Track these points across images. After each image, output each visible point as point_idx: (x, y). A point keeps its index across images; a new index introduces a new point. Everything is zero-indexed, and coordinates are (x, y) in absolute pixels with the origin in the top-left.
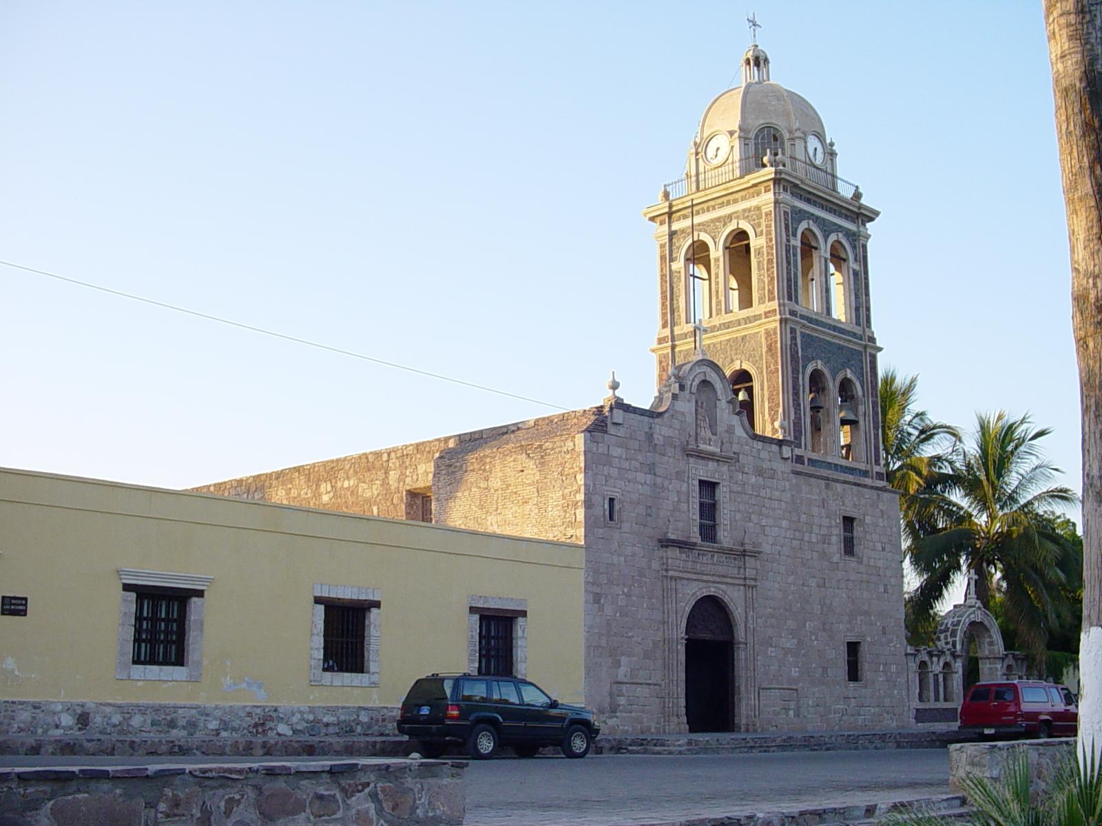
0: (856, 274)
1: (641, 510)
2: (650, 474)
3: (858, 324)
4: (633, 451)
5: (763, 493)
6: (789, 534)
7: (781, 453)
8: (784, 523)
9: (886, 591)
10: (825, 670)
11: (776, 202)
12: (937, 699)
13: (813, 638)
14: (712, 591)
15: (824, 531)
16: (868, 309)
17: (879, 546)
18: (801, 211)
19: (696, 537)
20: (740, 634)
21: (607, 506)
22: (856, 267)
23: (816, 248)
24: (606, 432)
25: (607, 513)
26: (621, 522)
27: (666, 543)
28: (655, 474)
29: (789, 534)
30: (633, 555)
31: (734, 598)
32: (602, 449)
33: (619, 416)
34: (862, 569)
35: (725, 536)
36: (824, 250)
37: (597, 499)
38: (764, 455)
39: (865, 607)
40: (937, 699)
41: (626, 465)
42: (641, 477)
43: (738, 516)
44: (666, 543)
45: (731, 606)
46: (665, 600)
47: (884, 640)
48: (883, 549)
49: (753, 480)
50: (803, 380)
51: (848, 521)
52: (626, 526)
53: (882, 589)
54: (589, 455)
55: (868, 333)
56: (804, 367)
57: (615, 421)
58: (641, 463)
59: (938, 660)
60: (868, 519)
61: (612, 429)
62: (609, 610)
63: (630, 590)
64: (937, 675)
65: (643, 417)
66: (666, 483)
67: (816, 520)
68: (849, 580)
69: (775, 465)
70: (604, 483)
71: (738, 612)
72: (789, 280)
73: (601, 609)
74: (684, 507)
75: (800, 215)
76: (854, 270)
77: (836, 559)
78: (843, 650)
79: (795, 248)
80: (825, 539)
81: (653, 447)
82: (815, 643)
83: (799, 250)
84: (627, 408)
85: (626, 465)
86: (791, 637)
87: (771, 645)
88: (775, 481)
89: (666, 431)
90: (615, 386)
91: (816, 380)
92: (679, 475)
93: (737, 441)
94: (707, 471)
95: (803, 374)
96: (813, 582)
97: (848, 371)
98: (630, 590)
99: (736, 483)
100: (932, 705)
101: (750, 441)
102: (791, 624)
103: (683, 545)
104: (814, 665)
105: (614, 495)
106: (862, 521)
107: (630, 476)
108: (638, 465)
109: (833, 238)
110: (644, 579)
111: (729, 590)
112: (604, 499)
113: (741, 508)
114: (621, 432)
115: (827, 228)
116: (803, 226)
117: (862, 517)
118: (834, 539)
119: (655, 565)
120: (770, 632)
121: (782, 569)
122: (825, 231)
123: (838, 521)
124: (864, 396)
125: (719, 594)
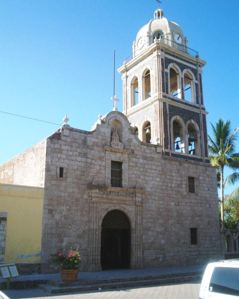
0: (196, 85)
1: (78, 173)
2: (84, 157)
3: (197, 103)
4: (75, 148)
5: (146, 167)
6: (160, 183)
7: (156, 150)
8: (158, 179)
9: (210, 207)
11: (158, 56)
13: (173, 227)
14: (117, 207)
15: (179, 182)
16: (202, 98)
17: (206, 189)
18: (170, 59)
20: (133, 226)
21: (58, 171)
22: (197, 82)
23: (178, 74)
24: (60, 139)
25: (59, 174)
26: (67, 178)
27: (91, 186)
28: (87, 158)
29: (160, 183)
30: (73, 192)
32: (57, 146)
34: (198, 198)
36: (181, 75)
37: (53, 168)
38: (148, 151)
41: (71, 153)
42: (79, 159)
43: (133, 176)
44: (91, 186)
45: (129, 215)
46: (90, 212)
48: (209, 190)
49: (141, 161)
50: (170, 122)
51: (191, 179)
52: (69, 180)
53: (208, 206)
54: (49, 149)
55: (202, 106)
57: (64, 134)
58: (79, 153)
59: (236, 234)
60: (201, 178)
62: (57, 217)
63: (70, 207)
64: (235, 240)
65: (81, 134)
66: (93, 162)
68: (191, 202)
69: (153, 155)
71: (132, 217)
72: (163, 84)
73: (53, 216)
75: (170, 61)
76: (195, 83)
77: (185, 193)
78: (189, 232)
79: (167, 73)
80: (179, 186)
81: (88, 147)
82: (174, 229)
84: (72, 130)
85: (71, 153)
86: (161, 226)
87: (150, 231)
88: (153, 162)
89: (94, 140)
90: (67, 120)
91: (176, 125)
92: (101, 158)
93: (133, 145)
94: (116, 157)
95: (170, 120)
96: (173, 204)
97: (192, 121)
98: (70, 207)
99: (132, 162)
101: (140, 145)
102: (161, 221)
103: (101, 187)
104: (173, 239)
105: (62, 166)
106: (198, 179)
107: (73, 158)
108: (77, 154)
109: (185, 71)
110: (79, 203)
111: (127, 207)
112: (57, 167)
113: (135, 172)
116: (171, 66)
117: (198, 177)
118: (184, 186)
119: (85, 196)
120: (150, 225)
121: (157, 198)
122: (182, 68)
123: (186, 178)
124: (200, 130)
125: (122, 209)
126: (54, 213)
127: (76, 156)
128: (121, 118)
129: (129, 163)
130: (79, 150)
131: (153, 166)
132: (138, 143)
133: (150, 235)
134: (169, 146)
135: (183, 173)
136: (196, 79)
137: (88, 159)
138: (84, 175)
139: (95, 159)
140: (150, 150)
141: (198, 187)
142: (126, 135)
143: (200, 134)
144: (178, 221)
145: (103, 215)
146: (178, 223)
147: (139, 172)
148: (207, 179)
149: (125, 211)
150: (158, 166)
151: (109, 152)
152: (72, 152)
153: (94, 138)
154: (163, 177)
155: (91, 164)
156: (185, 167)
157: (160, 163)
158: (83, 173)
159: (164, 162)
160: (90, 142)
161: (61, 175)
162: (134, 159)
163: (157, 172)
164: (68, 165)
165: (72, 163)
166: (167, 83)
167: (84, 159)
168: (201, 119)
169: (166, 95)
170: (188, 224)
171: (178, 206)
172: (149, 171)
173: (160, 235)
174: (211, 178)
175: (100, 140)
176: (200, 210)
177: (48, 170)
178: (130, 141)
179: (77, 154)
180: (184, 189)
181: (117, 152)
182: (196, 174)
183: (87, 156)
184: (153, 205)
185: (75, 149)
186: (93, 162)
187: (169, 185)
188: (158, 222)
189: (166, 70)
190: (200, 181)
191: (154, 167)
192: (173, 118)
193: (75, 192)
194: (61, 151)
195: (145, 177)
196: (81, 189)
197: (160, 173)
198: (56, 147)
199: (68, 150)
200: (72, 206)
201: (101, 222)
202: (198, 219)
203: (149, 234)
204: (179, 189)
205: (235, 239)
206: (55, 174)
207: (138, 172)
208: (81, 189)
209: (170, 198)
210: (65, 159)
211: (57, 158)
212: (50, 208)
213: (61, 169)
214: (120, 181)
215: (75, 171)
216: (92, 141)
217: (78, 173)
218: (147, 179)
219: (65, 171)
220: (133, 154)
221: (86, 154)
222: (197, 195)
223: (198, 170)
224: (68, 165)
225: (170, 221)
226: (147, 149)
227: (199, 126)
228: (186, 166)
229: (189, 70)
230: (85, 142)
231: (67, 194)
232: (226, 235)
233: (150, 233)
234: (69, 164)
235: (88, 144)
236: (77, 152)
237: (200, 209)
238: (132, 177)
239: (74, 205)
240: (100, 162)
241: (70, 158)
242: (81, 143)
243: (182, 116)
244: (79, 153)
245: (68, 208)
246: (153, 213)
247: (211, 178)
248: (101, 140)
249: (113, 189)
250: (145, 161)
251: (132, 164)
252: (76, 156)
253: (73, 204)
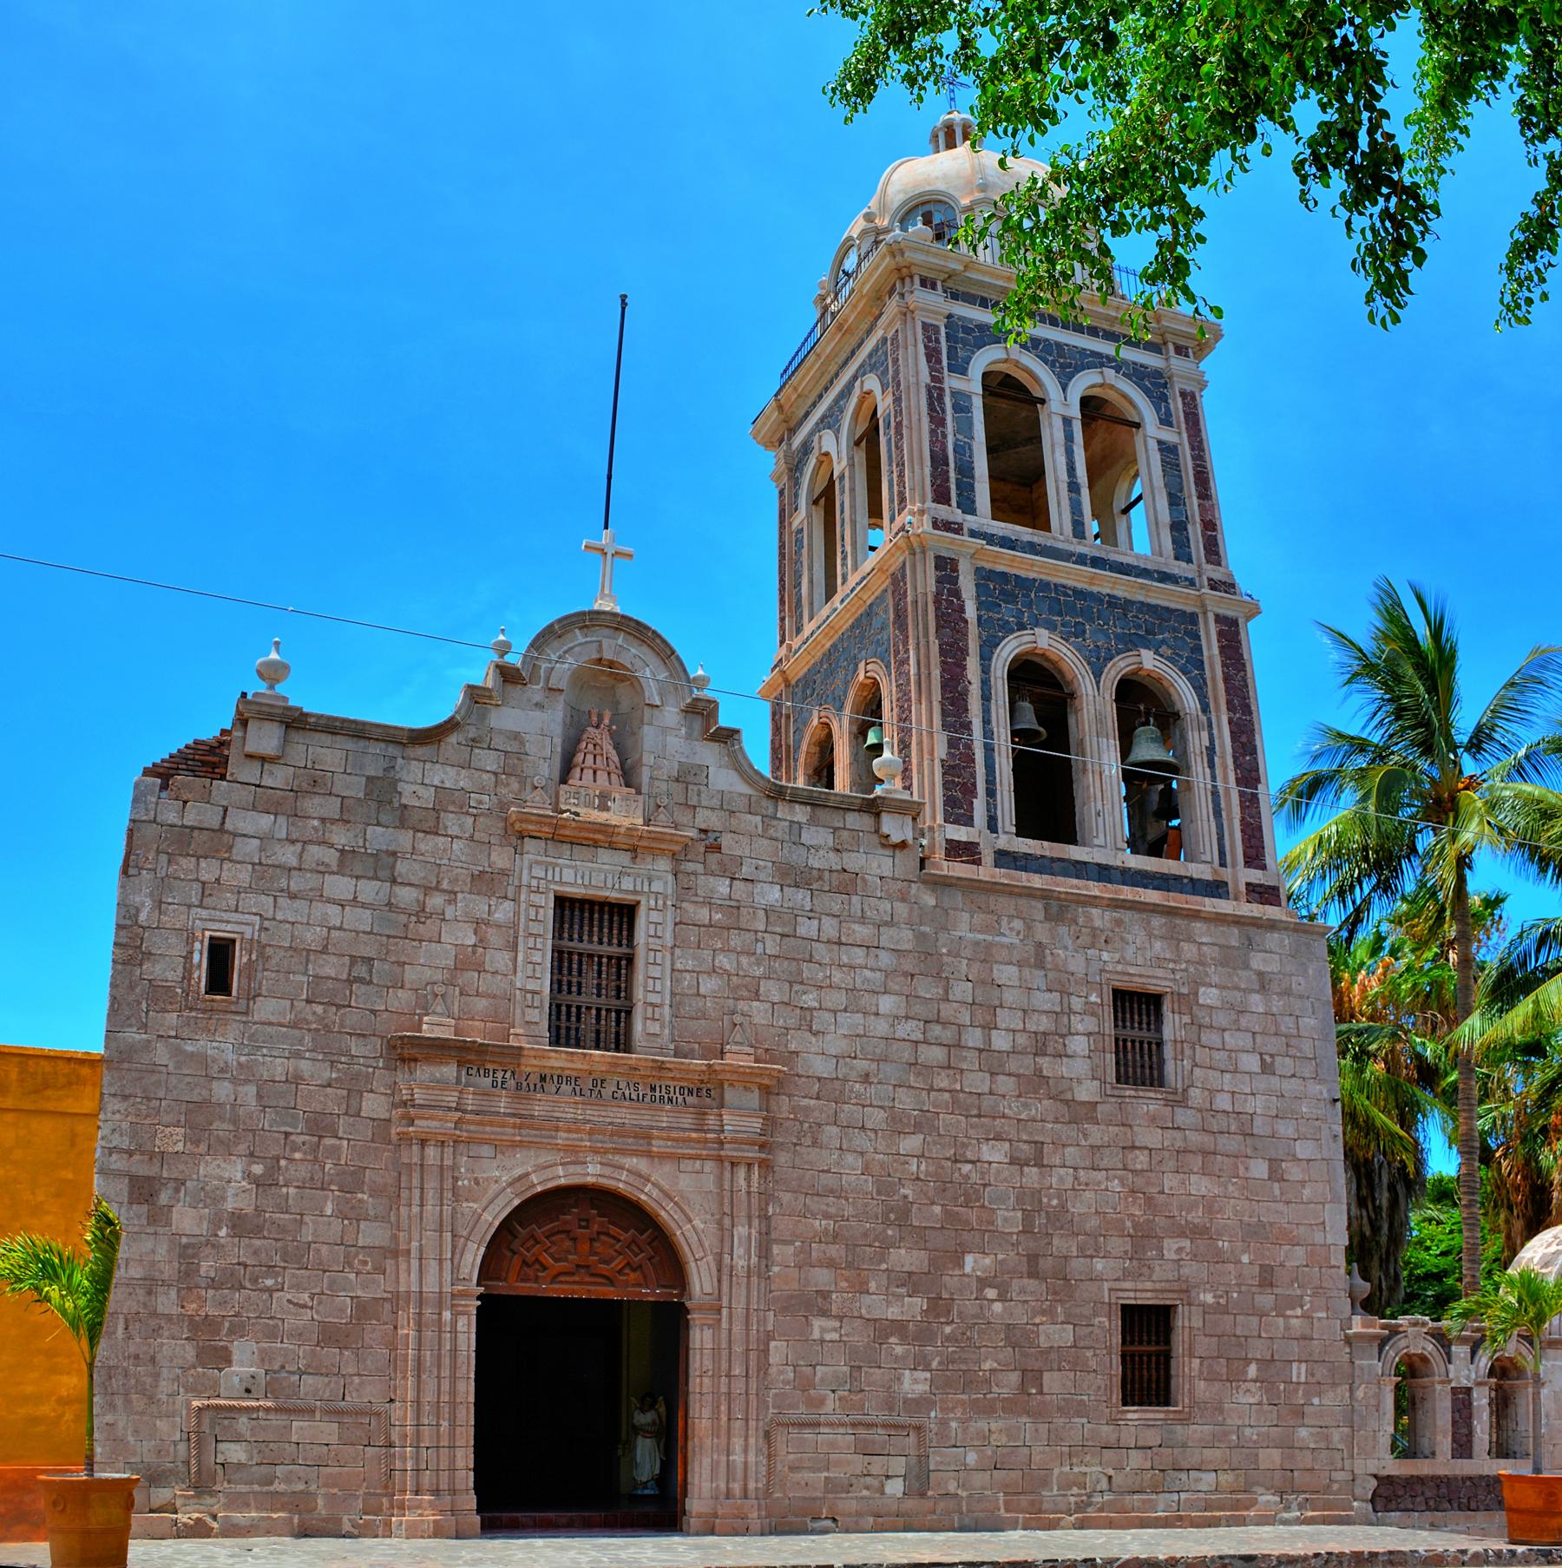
4: (316, 823)
5: (807, 928)
8: (887, 1004)
9: (1275, 1175)
10: (1031, 1377)
12: (1463, 1447)
14: (592, 1173)
16: (1210, 526)
17: (1251, 1062)
19: (529, 1026)
21: (201, 958)
22: (1168, 436)
23: (1043, 401)
26: (252, 996)
28: (394, 881)
30: (295, 1080)
31: (683, 1195)
33: (265, 738)
34: (1183, 1117)
38: (816, 836)
39: (1197, 1216)
40: (1463, 1447)
41: (288, 855)
42: (340, 886)
43: (708, 985)
45: (667, 1214)
46: (405, 1194)
47: (1265, 1300)
48: (1267, 1069)
50: (986, 670)
51: (1137, 1007)
53: (1260, 1169)
56: (988, 648)
58: (342, 851)
59: (1473, 1353)
60: (1208, 996)
61: (241, 770)
63: (273, 1165)
64: (1469, 1390)
65: (362, 743)
67: (1009, 997)
68: (1134, 1147)
69: (854, 861)
70: (195, 901)
71: (693, 1231)
74: (501, 960)
76: (1160, 442)
78: (1109, 1328)
80: (1041, 1045)
82: (998, 1307)
83: (978, 404)
84: (295, 722)
85: (288, 855)
86: (903, 1291)
87: (825, 1313)
88: (855, 899)
89: (444, 776)
92: (487, 882)
93: (715, 802)
99: (708, 903)
100: (1442, 1464)
101: (765, 803)
102: (906, 1258)
104: (987, 1365)
105: (224, 931)
106: (1187, 1002)
108: (331, 857)
110: (328, 1141)
111: (661, 1174)
113: (724, 961)
114: (277, 777)
117: (1185, 990)
118: (1078, 1045)
120: (822, 1277)
121: (877, 1117)
122: (1062, 366)
123: (1094, 998)
124: (1205, 709)
125: (621, 1183)
126: (164, 1198)
127: (322, 870)
128: (632, 654)
129: (684, 905)
130: (341, 837)
131: (856, 927)
132: (744, 789)
133: (822, 1341)
134: (979, 805)
135: (1077, 965)
136: (1166, 421)
137: (397, 889)
138: (370, 982)
139: (445, 885)
140: (836, 829)
141: (1188, 1052)
142: (665, 741)
143: (1205, 735)
144: (1033, 1259)
145: (493, 1218)
146: (1033, 1274)
147: (753, 959)
148: (1256, 1002)
149: (646, 1195)
150: (890, 923)
151: (542, 843)
152: (299, 846)
153: (448, 769)
154: (927, 989)
155: (421, 913)
156: (1093, 929)
157: (902, 909)
158: (361, 971)
159: (932, 902)
160: (421, 790)
161: (219, 980)
162: (722, 887)
163: (886, 959)
164: (266, 924)
165: (289, 910)
166: (963, 450)
167: (370, 890)
168: (1211, 649)
169: (953, 513)
170: (1113, 1281)
171: (1035, 1170)
172: (821, 951)
173: (892, 1340)
174: (1287, 992)
175: (485, 776)
176: (1203, 1191)
178: (688, 776)
179: (326, 860)
180: (1083, 1062)
181: (596, 844)
182: (1173, 971)
183: (393, 867)
184: (850, 1158)
185: (315, 828)
186: (436, 901)
187: (974, 1038)
188: (884, 1266)
189: (952, 382)
190: (1202, 1015)
191: (862, 932)
192: (1009, 649)
193: (306, 1075)
194: (219, 841)
195: (796, 987)
196: (343, 1059)
197: (908, 965)
198: (190, 819)
199: (265, 839)
200: (283, 1163)
201: (473, 1256)
202: (1180, 1250)
203: (816, 1335)
204: (1045, 1062)
205: (1465, 1383)
206: (174, 975)
207: (744, 960)
208: (343, 1059)
209: (979, 1116)
210: (249, 889)
211: (197, 886)
212: (141, 1168)
213: (221, 952)
214: (625, 1014)
215: (308, 961)
216: (436, 782)
217: (331, 967)
218: (809, 1000)
219: (245, 960)
220: (713, 858)
221: (391, 859)
222: (1179, 1100)
223: (1189, 950)
224: (266, 924)
225: (969, 1260)
226: (813, 821)
227: (1200, 688)
228: (1098, 923)
229: (1110, 373)
230: (382, 792)
231: (252, 1090)
232: (1393, 1354)
233: (823, 1330)
234: (270, 914)
235: (404, 801)
236: (332, 846)
237: (1201, 1186)
238: (702, 991)
239: (297, 1156)
240: (480, 907)
241: (284, 884)
242: (361, 795)
243: (1073, 633)
244: (342, 851)
245: (258, 1169)
246: (849, 1211)
247: (1287, 992)
248: (496, 774)
249: (561, 1059)
250: (801, 897)
251: (703, 915)
252: (322, 870)
253: (294, 1150)
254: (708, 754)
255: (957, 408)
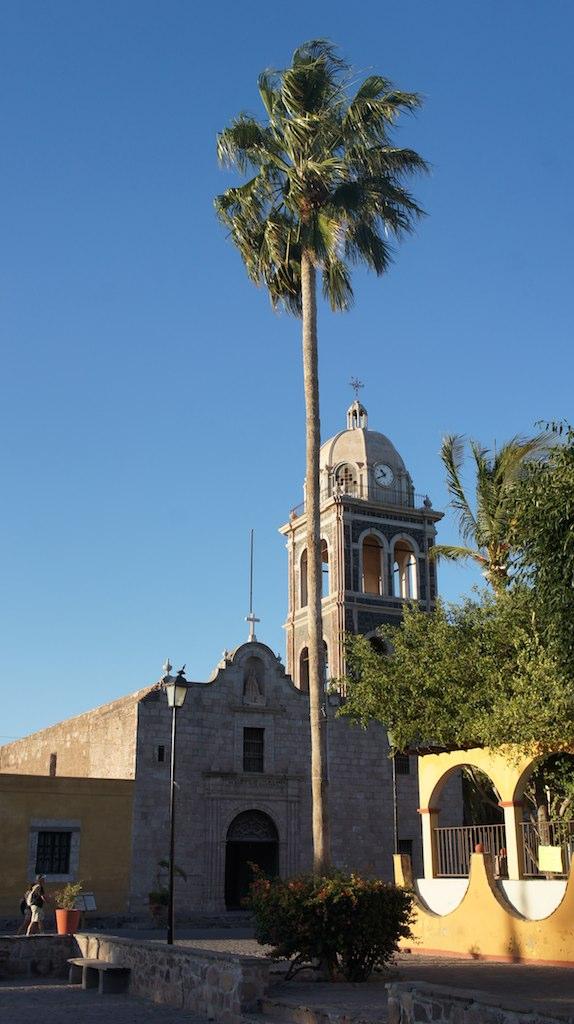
13: (360, 837)
14: (254, 806)
19: (238, 766)
20: (282, 836)
21: (156, 752)
32: (154, 712)
35: (269, 766)
36: (388, 548)
43: (283, 751)
44: (209, 774)
55: (431, 603)
71: (280, 821)
75: (365, 525)
79: (356, 552)
83: (361, 552)
109: (397, 538)
113: (288, 744)
115: (390, 532)
125: (262, 809)
126: (149, 818)
132: (293, 692)
142: (271, 680)
145: (229, 820)
158: (196, 753)
161: (161, 758)
177: (140, 751)
178: (277, 689)
181: (253, 712)
186: (213, 732)
187: (355, 762)
189: (354, 546)
198: (152, 714)
214: (261, 759)
220: (284, 714)
225: (354, 828)
249: (247, 775)
254: (282, 682)
255: (354, 555)
